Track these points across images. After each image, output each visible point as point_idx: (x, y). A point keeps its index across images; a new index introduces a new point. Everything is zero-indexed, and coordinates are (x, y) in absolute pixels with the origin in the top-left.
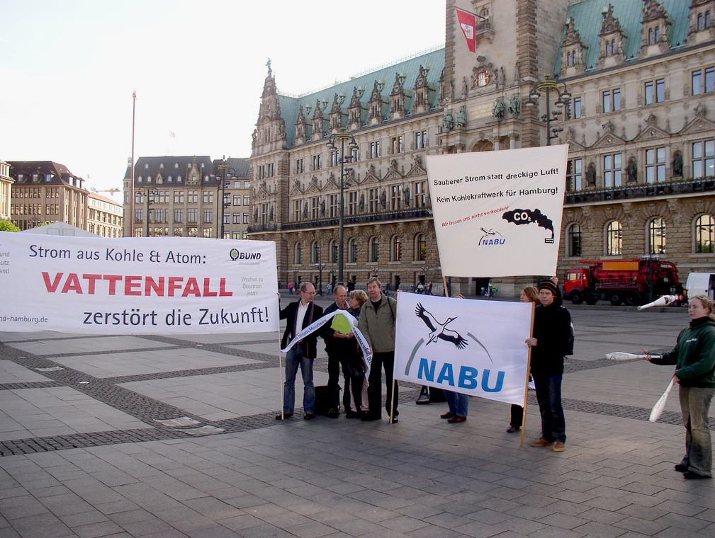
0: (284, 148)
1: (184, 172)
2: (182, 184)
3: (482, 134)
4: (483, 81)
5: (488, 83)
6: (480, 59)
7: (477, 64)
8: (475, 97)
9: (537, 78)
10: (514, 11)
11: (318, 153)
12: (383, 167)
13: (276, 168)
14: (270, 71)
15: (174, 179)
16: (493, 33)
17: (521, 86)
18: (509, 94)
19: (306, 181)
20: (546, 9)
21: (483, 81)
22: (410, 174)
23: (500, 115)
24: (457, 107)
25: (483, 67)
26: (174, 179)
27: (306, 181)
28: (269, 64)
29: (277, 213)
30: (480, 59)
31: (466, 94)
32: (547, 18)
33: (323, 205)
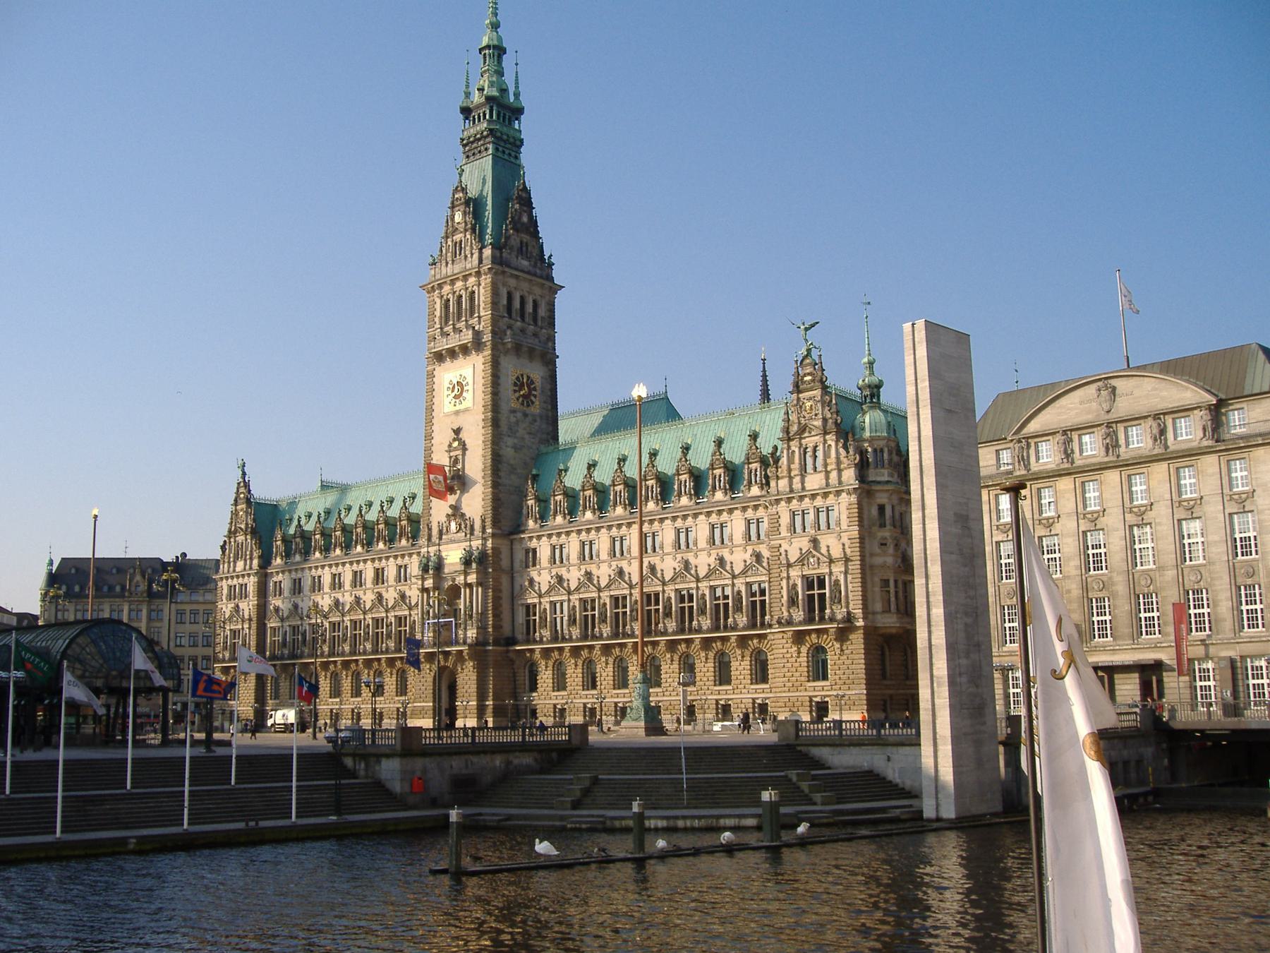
3: (454, 580)
7: (450, 511)
8: (447, 543)
10: (481, 466)
11: (299, 575)
12: (368, 598)
14: (244, 474)
18: (477, 544)
20: (512, 462)
21: (453, 526)
22: (393, 607)
23: (467, 562)
24: (432, 550)
31: (440, 538)
33: (304, 634)
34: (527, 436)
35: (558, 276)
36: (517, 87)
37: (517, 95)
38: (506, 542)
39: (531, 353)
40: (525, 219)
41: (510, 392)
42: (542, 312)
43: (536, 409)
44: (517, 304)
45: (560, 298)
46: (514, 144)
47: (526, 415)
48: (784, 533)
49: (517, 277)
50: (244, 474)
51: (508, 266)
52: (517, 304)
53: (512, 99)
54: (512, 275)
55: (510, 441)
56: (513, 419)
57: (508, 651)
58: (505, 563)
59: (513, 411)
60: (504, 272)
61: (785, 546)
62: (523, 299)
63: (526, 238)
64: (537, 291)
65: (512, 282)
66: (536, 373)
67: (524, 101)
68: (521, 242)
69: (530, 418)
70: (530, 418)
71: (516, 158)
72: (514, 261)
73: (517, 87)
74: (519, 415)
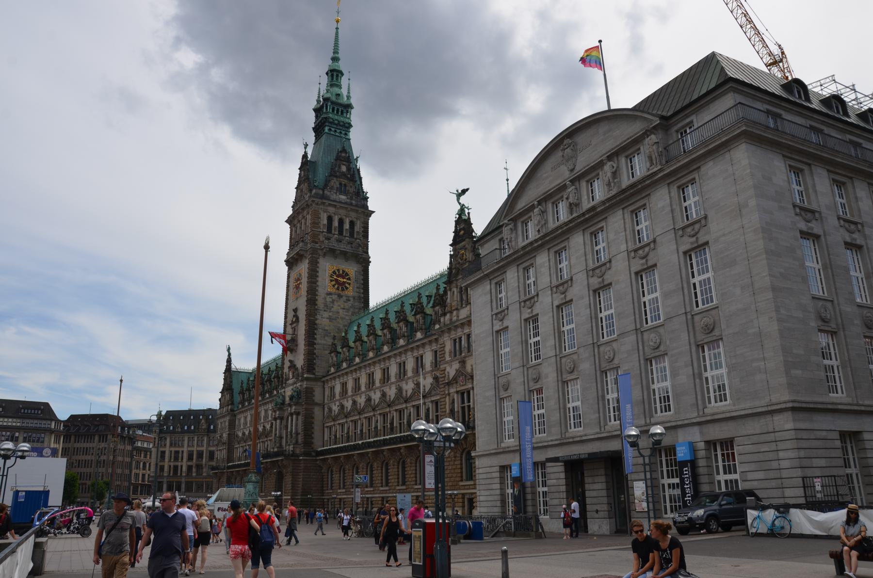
0: (232, 410)
1: (197, 421)
2: (193, 432)
4: (291, 376)
5: (293, 377)
6: (290, 361)
9: (314, 374)
13: (227, 424)
14: (229, 355)
15: (189, 427)
16: (297, 345)
17: (302, 381)
19: (240, 434)
23: (292, 398)
25: (293, 366)
26: (189, 427)
27: (240, 434)
28: (229, 350)
29: (226, 456)
30: (290, 361)
32: (326, 333)
34: (341, 311)
35: (371, 206)
36: (349, 93)
37: (348, 97)
38: (320, 384)
39: (345, 255)
40: (344, 169)
41: (327, 281)
42: (358, 227)
43: (351, 292)
44: (336, 223)
45: (372, 221)
46: (344, 126)
47: (340, 296)
48: (448, 358)
49: (335, 206)
50: (229, 355)
51: (329, 200)
52: (336, 223)
53: (346, 98)
54: (330, 205)
55: (326, 315)
56: (329, 299)
57: (317, 460)
58: (318, 398)
59: (330, 294)
60: (324, 203)
61: (448, 369)
62: (341, 222)
63: (344, 181)
64: (353, 215)
65: (331, 210)
66: (352, 269)
67: (353, 101)
68: (341, 184)
69: (344, 298)
70: (344, 298)
71: (346, 134)
72: (334, 197)
73: (349, 93)
74: (335, 297)
